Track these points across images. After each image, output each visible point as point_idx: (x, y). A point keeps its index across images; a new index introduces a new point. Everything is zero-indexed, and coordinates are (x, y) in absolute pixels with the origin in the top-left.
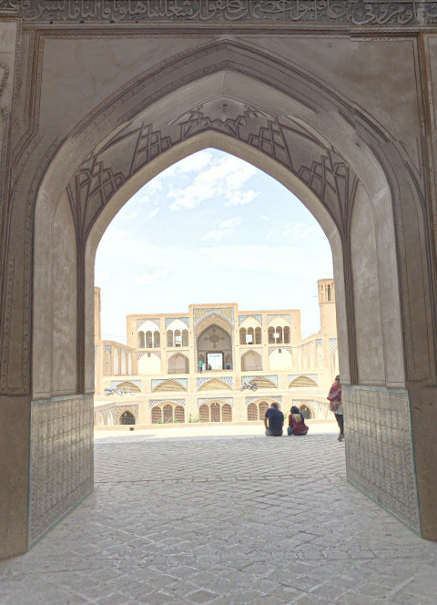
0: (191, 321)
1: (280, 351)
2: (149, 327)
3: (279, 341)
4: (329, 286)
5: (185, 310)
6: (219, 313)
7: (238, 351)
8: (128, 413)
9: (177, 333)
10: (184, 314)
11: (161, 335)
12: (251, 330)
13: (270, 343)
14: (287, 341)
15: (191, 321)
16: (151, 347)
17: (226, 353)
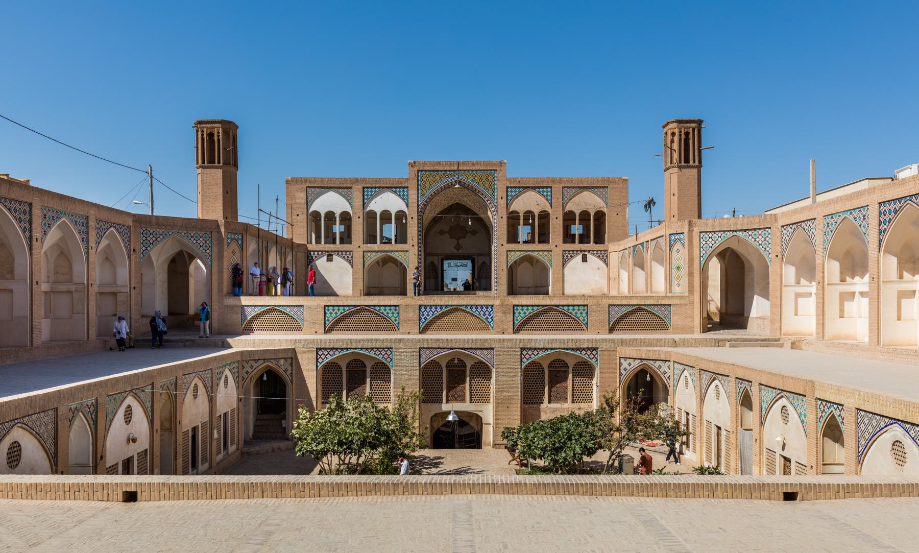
0: (413, 194)
1: (585, 259)
2: (330, 202)
3: (584, 239)
4: (687, 134)
6: (469, 181)
7: (502, 254)
8: (270, 372)
9: (386, 217)
10: (399, 180)
12: (529, 214)
13: (564, 242)
14: (599, 239)
17: (479, 260)
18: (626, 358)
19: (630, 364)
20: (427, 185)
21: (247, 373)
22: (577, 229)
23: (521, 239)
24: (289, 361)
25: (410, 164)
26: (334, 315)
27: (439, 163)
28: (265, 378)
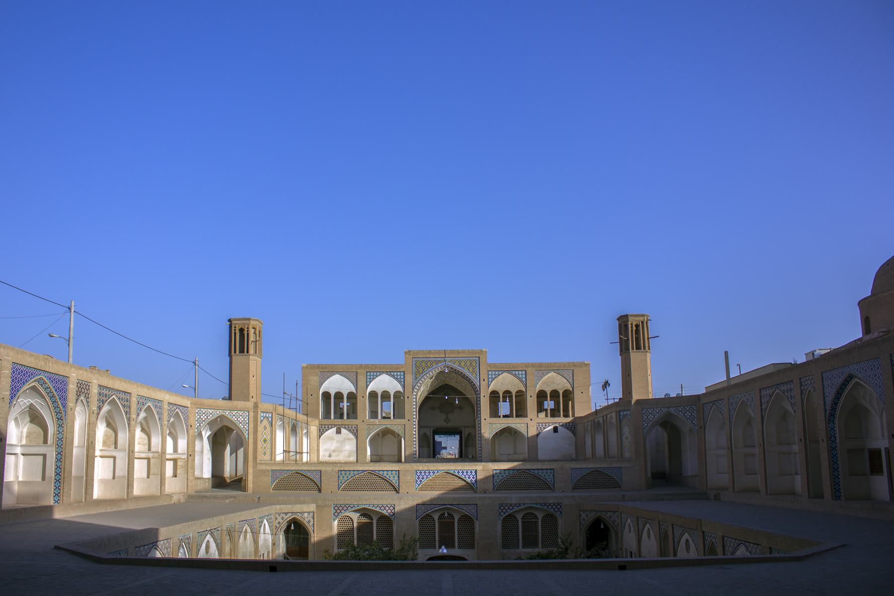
0: (409, 378)
5: (399, 359)
6: (456, 366)
9: (386, 396)
11: (359, 399)
12: (507, 393)
15: (409, 378)
16: (341, 416)
18: (584, 511)
19: (587, 516)
20: (421, 370)
21: (279, 523)
22: (549, 404)
23: (502, 413)
24: (311, 514)
25: (406, 353)
26: (346, 478)
27: (430, 352)
28: (292, 528)
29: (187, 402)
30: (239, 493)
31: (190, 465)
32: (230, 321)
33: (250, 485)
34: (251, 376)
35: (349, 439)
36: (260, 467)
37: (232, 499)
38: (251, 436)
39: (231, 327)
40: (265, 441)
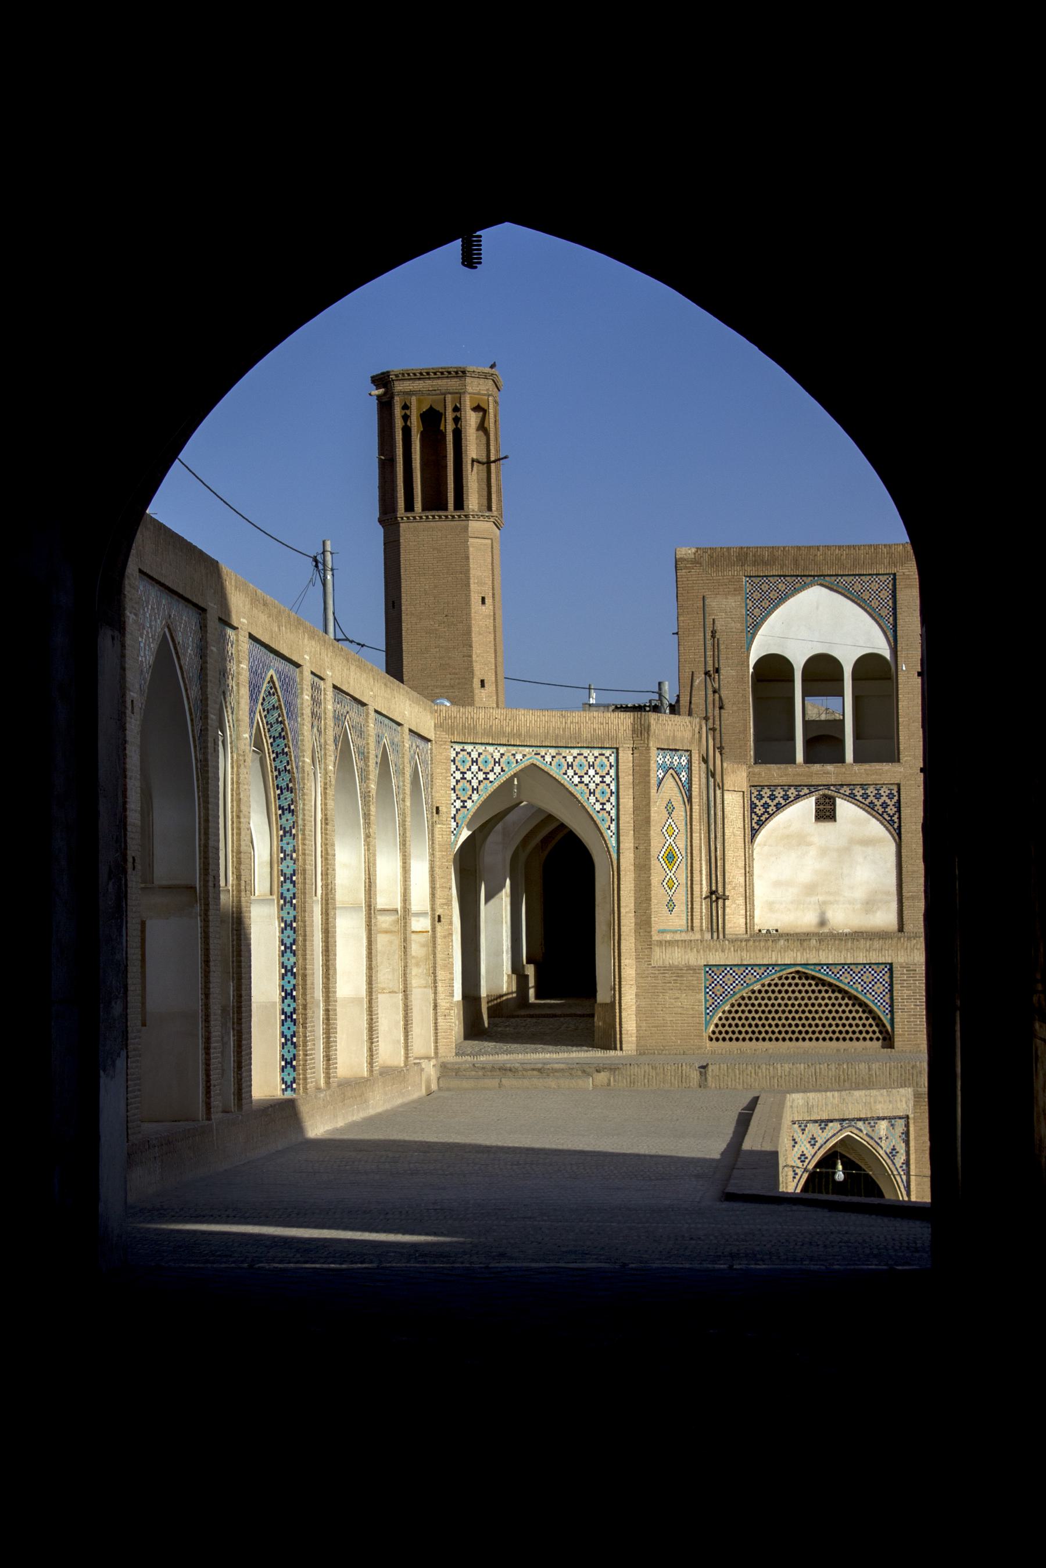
21: (803, 1157)
24: (900, 1124)
29: (427, 725)
30: (598, 1054)
31: (440, 956)
32: (382, 380)
33: (630, 1024)
34: (475, 599)
35: (868, 842)
36: (661, 957)
37: (602, 1077)
38: (628, 843)
39: (385, 406)
40: (671, 857)
